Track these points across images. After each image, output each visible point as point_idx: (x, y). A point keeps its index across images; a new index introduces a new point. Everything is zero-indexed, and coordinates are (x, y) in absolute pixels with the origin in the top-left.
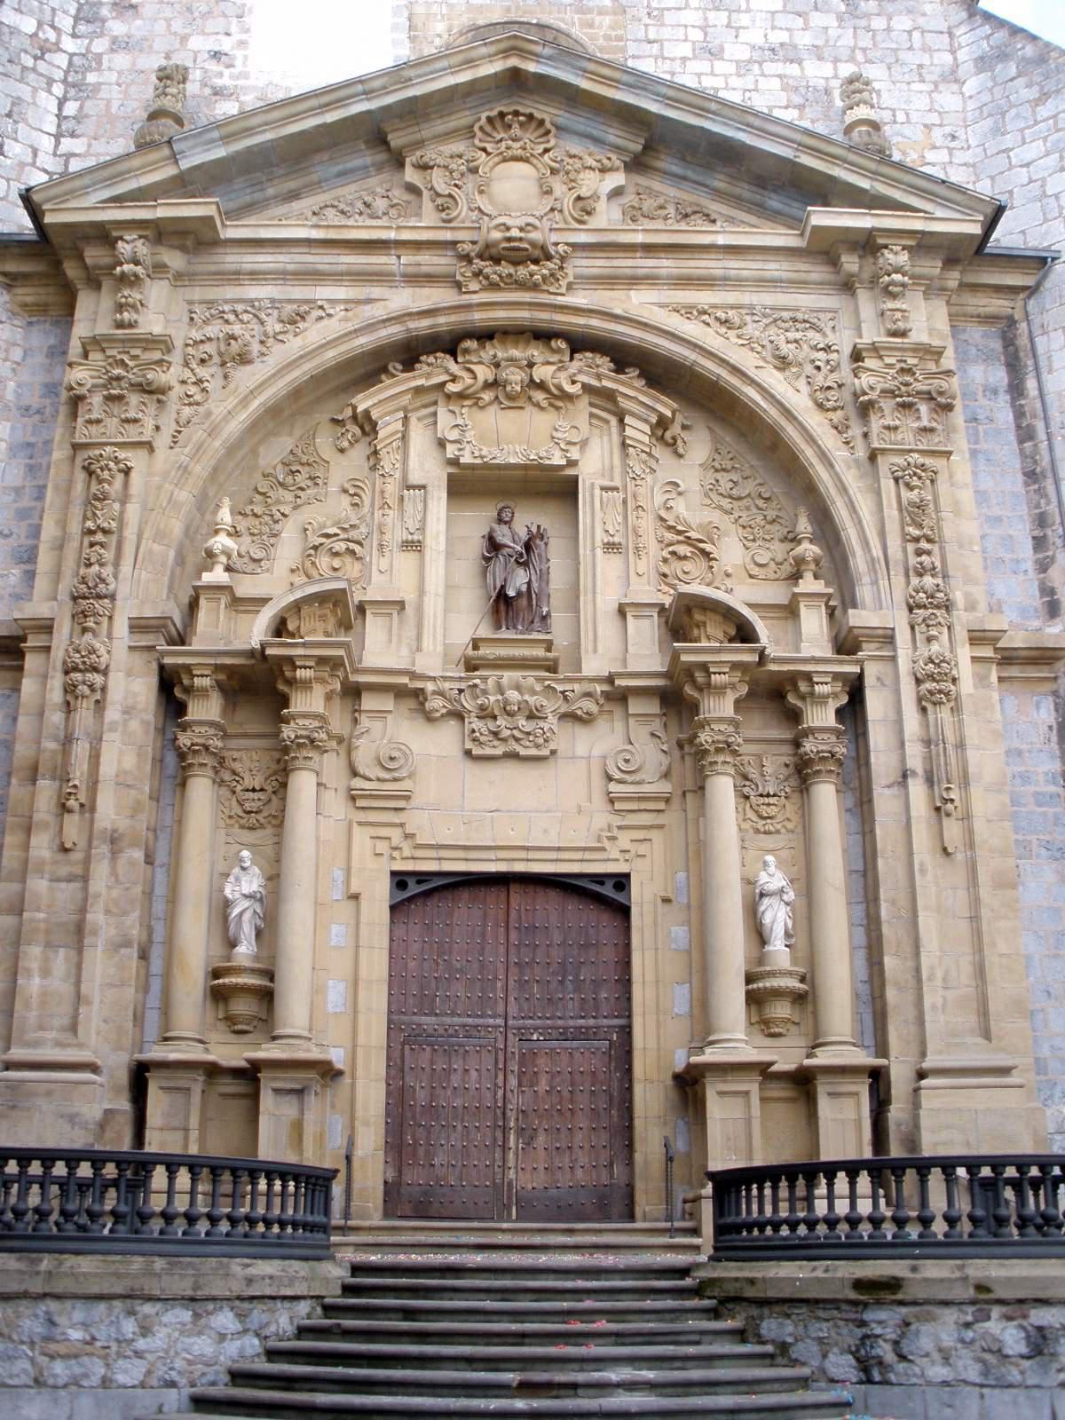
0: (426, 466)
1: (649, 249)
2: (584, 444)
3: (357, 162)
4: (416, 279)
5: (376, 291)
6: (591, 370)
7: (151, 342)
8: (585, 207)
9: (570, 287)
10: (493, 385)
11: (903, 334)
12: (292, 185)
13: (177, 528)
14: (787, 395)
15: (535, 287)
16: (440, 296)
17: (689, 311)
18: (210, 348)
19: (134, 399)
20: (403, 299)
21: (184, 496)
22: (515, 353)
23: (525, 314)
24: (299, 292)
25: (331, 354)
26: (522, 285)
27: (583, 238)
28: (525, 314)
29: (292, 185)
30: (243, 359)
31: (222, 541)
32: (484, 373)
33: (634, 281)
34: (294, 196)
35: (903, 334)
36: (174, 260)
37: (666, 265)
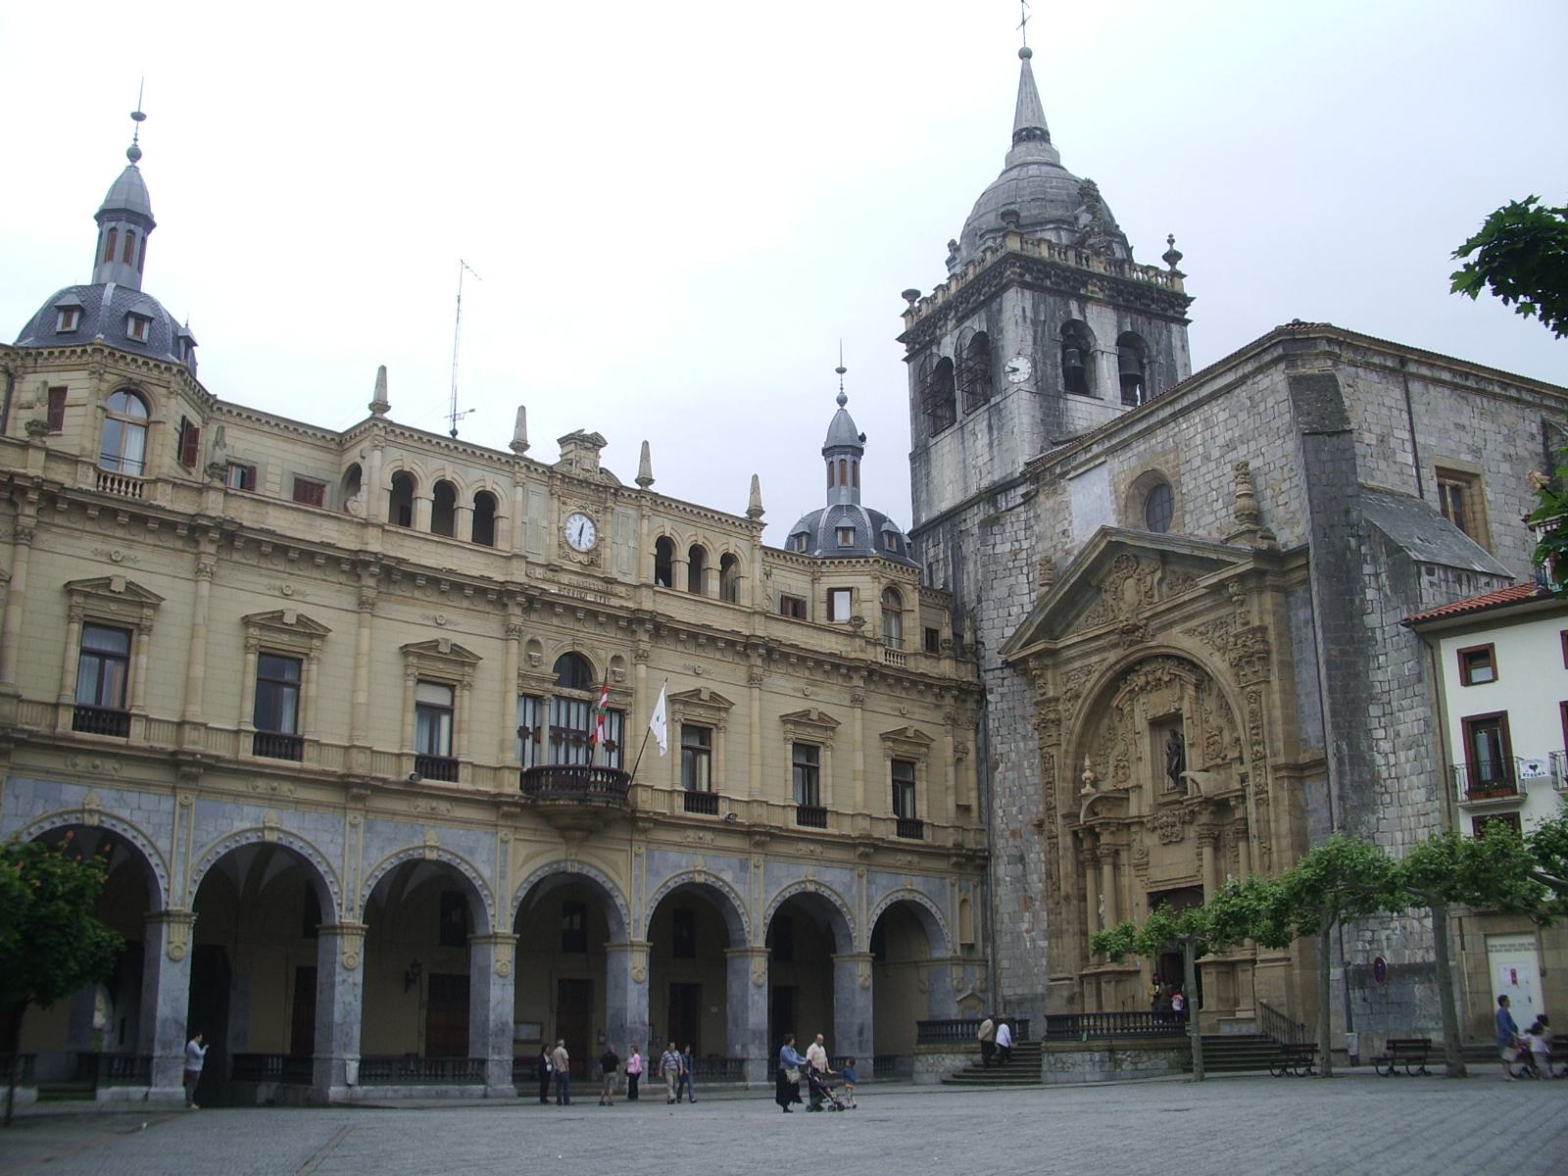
0: (1141, 723)
1: (1169, 610)
2: (1181, 699)
3: (1088, 596)
4: (1114, 646)
5: (1106, 655)
6: (1172, 667)
7: (1049, 701)
8: (1149, 594)
9: (1153, 636)
10: (1148, 683)
11: (1247, 623)
12: (1075, 612)
13: (1069, 774)
14: (1217, 664)
15: (1142, 642)
16: (1119, 653)
17: (1191, 632)
18: (1069, 694)
19: (1050, 724)
20: (1112, 656)
21: (1069, 761)
22: (1148, 669)
23: (1142, 653)
24: (1086, 662)
25: (1096, 689)
26: (1137, 642)
27: (1147, 614)
28: (1142, 653)
29: (1075, 612)
30: (1078, 696)
31: (1087, 774)
32: (1143, 679)
33: (1171, 624)
34: (1078, 616)
35: (1247, 623)
36: (1048, 661)
37: (1176, 614)
